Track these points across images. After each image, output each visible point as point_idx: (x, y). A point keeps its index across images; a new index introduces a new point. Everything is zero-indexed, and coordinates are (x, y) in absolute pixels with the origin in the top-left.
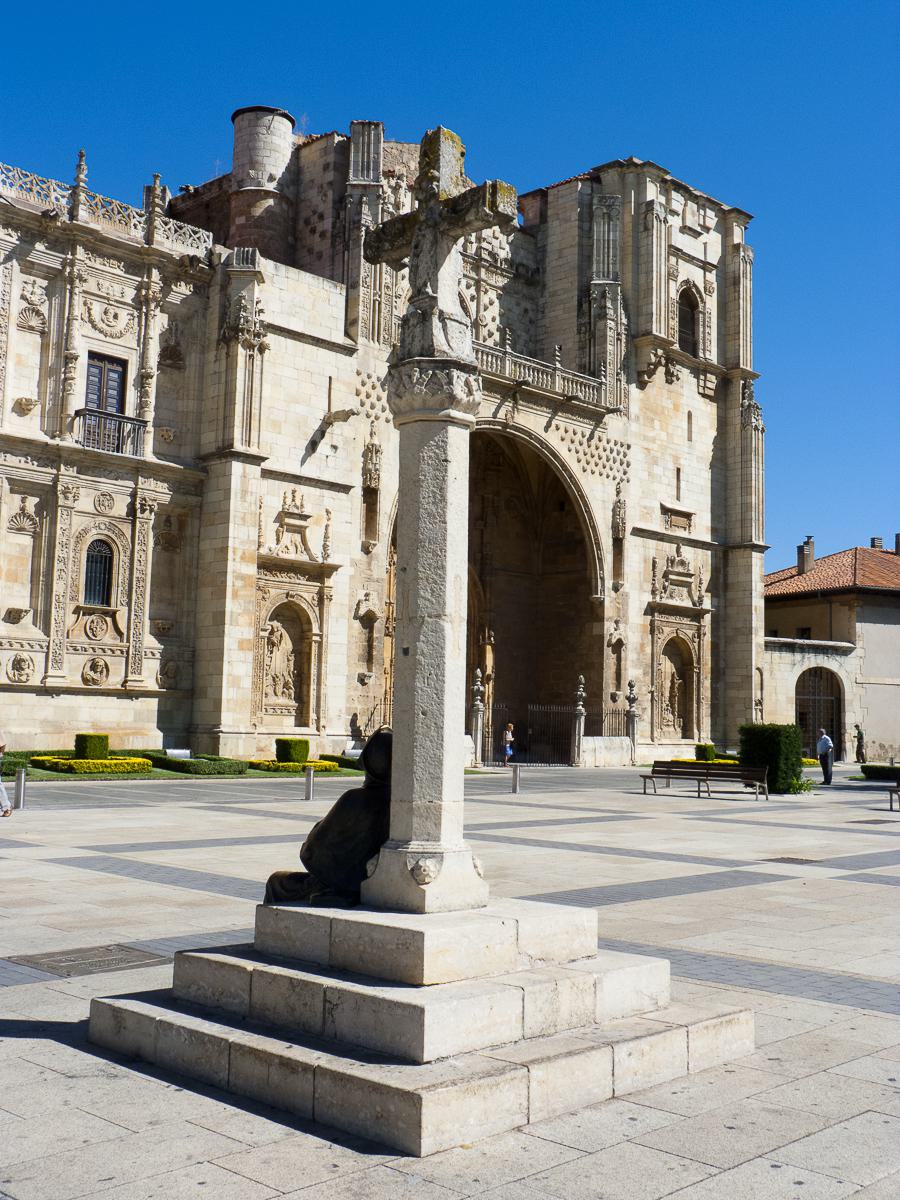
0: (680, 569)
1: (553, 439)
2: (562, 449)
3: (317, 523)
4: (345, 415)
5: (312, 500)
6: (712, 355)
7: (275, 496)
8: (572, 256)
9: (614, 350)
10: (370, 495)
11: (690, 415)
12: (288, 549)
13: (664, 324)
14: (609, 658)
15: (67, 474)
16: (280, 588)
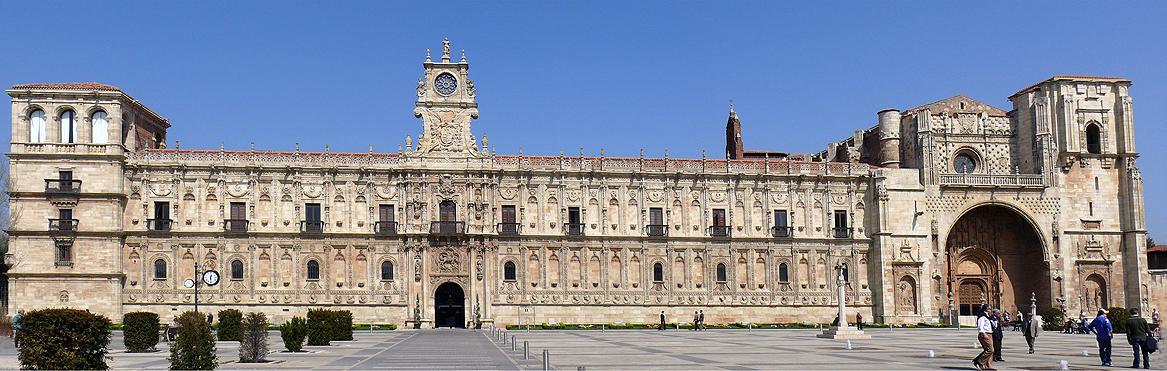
0: (1095, 245)
1: (1017, 204)
2: (1023, 207)
3: (915, 249)
4: (921, 214)
5: (911, 242)
6: (1112, 149)
7: (898, 243)
8: (1029, 123)
9: (1049, 160)
10: (935, 237)
11: (1096, 178)
12: (905, 259)
13: (1077, 143)
14: (1054, 285)
15: (832, 246)
16: (902, 271)
